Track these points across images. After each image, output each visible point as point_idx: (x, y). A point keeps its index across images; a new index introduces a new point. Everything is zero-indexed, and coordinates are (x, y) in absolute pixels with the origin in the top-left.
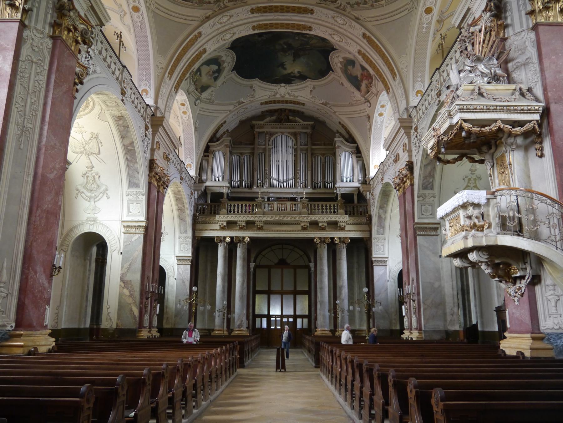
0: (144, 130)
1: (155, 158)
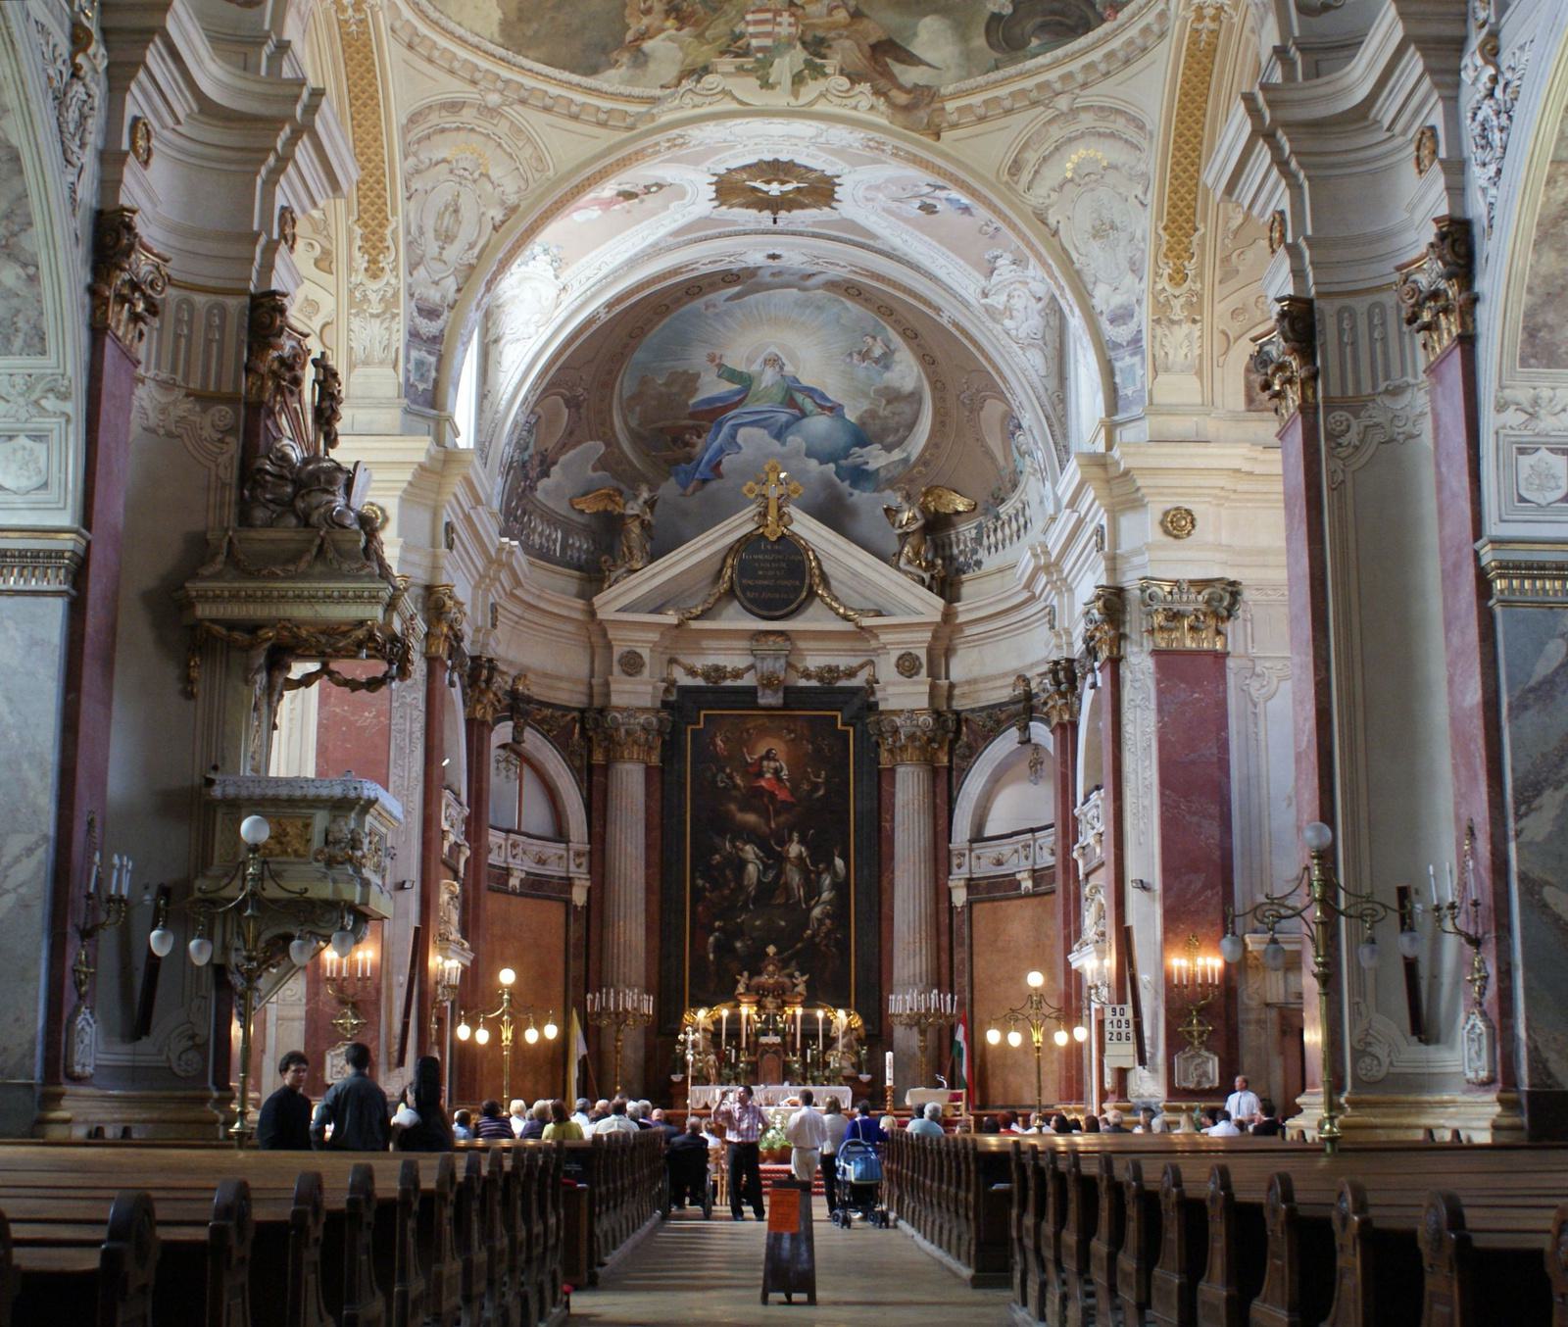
0: (64, 47)
1: (124, 200)
